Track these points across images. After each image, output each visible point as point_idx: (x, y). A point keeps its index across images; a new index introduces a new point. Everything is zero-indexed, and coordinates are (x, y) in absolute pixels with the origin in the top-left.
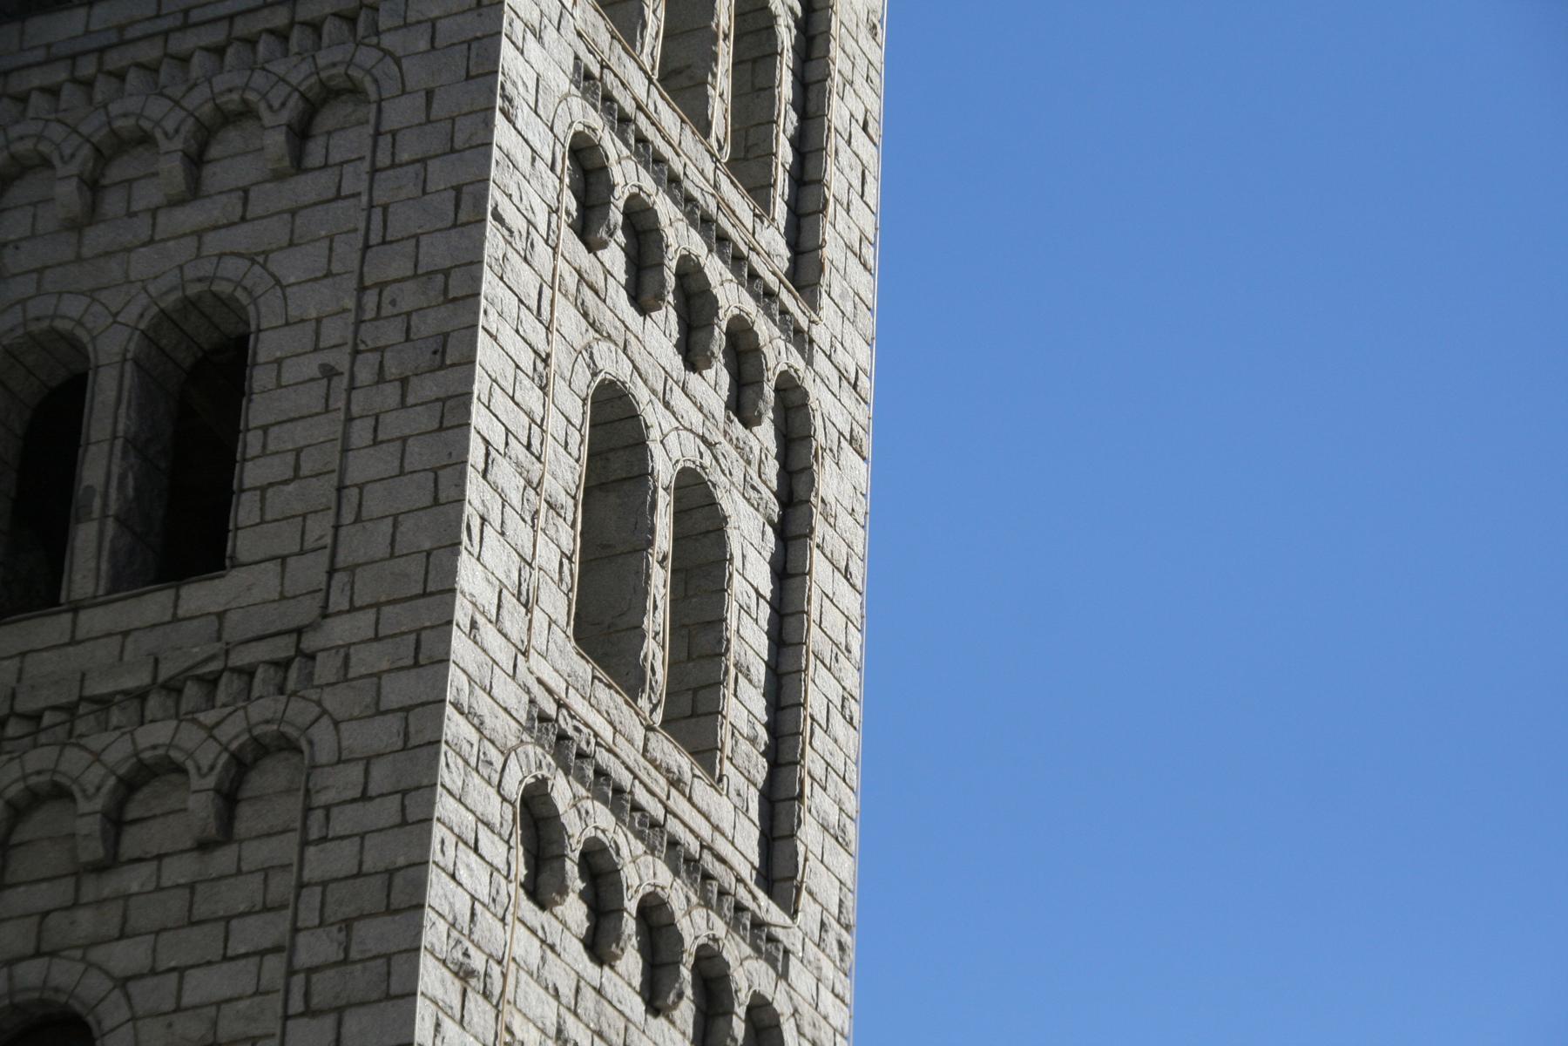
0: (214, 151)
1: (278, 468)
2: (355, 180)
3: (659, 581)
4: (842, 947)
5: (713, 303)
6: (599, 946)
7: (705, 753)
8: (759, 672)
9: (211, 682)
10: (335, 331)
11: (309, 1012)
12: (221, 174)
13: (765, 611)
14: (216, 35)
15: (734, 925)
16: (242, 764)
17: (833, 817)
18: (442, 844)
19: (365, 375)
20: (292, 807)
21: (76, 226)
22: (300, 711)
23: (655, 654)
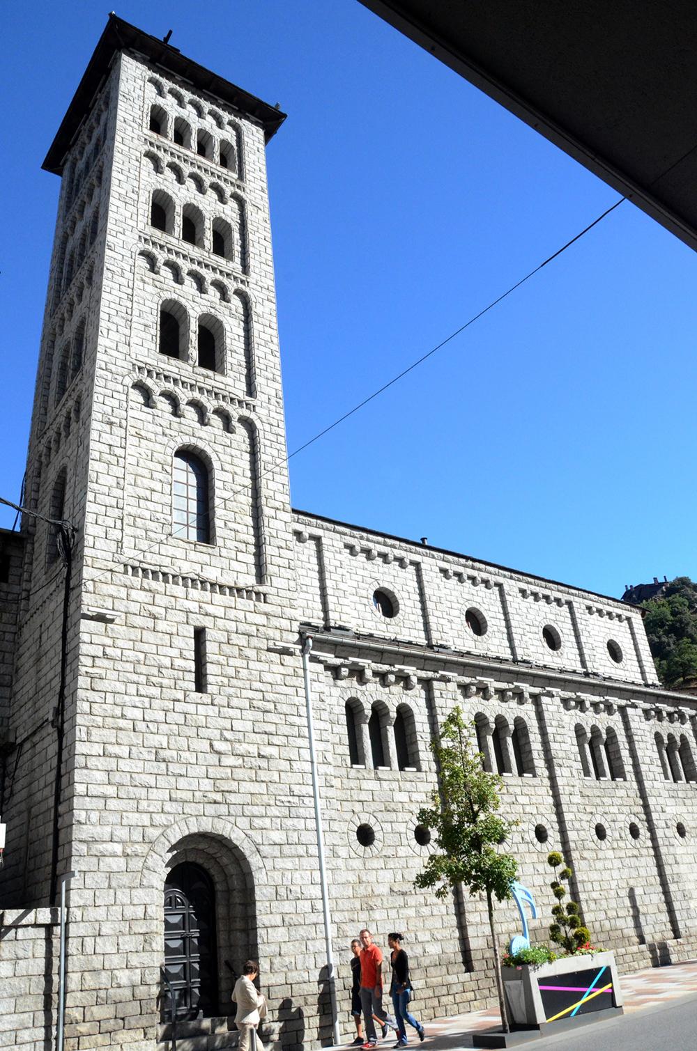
4: (278, 403)
5: (204, 278)
13: (242, 339)
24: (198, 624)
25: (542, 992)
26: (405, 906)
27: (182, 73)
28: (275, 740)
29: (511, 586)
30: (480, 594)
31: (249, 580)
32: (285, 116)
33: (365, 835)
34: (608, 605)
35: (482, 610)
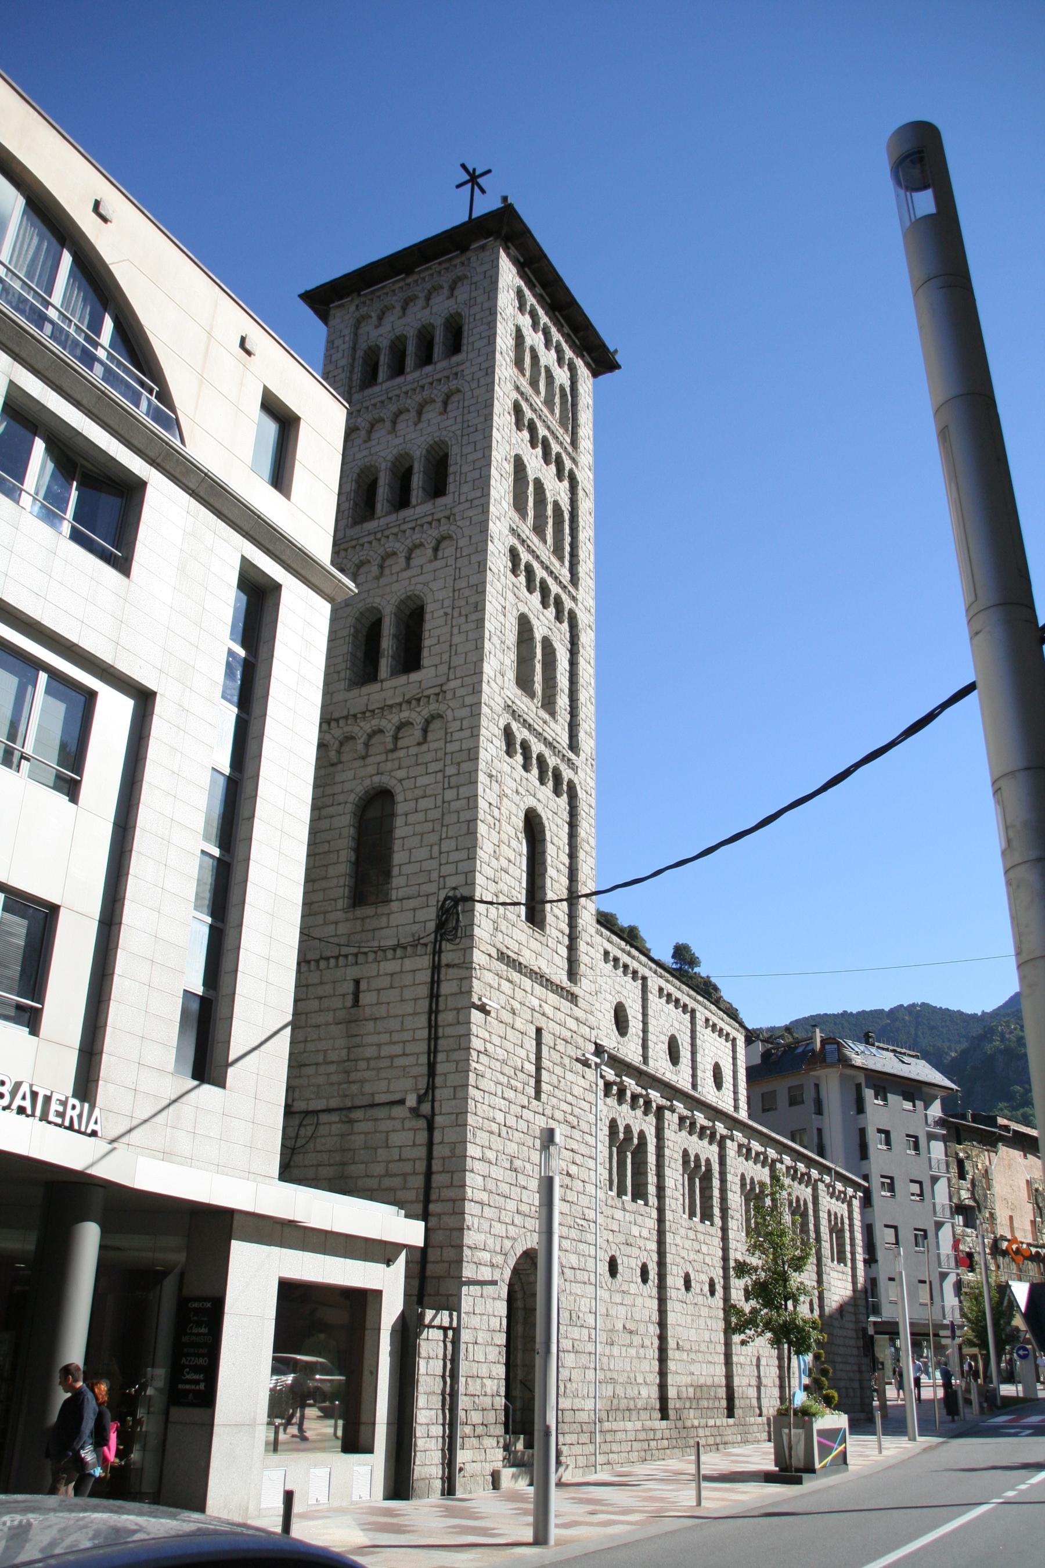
0: (413, 555)
1: (434, 641)
2: (451, 561)
3: (539, 668)
5: (550, 591)
6: (526, 767)
7: (553, 714)
8: (567, 691)
9: (419, 700)
10: (447, 603)
11: (450, 788)
12: (414, 562)
13: (567, 674)
14: (412, 524)
15: (563, 760)
16: (428, 722)
17: (588, 730)
18: (483, 742)
19: (456, 614)
20: (442, 733)
21: (377, 578)
22: (443, 707)
23: (538, 688)
24: (539, 1025)
25: (819, 1442)
26: (630, 1345)
27: (544, 286)
28: (578, 1159)
29: (655, 982)
30: (628, 986)
31: (560, 976)
32: (618, 367)
33: (613, 1268)
34: (722, 1019)
35: (627, 1006)
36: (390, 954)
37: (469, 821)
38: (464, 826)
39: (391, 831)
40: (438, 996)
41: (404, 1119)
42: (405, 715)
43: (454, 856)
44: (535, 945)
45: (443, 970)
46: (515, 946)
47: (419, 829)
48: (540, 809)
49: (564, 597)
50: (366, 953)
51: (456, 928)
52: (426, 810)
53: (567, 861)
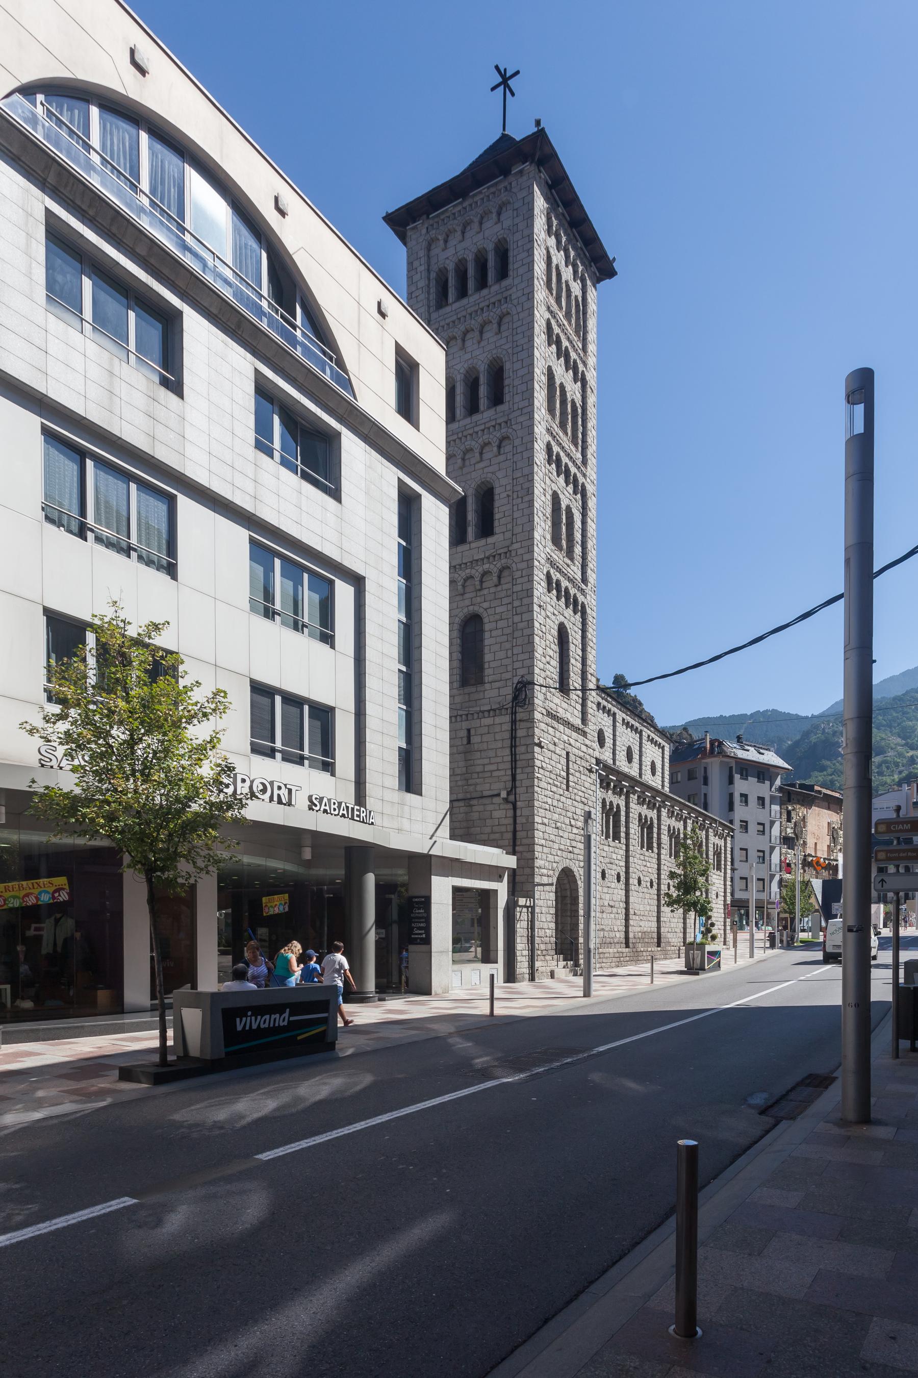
0: (484, 451)
1: (501, 515)
2: (510, 456)
3: (564, 528)
6: (558, 598)
7: (572, 559)
8: (580, 542)
9: (494, 556)
10: (508, 488)
11: (516, 614)
12: (485, 456)
14: (482, 427)
15: (578, 590)
16: (501, 571)
17: (592, 568)
18: (536, 585)
19: (515, 497)
20: (510, 579)
21: (461, 468)
22: (510, 561)
23: (564, 543)
31: (577, 722)
36: (486, 714)
37: (529, 635)
38: (526, 638)
39: (482, 640)
40: (515, 738)
41: (500, 804)
42: (486, 566)
43: (521, 657)
44: (565, 705)
45: (518, 723)
46: (554, 707)
47: (499, 640)
48: (566, 622)
49: (579, 475)
50: (472, 714)
51: (525, 700)
52: (502, 628)
53: (580, 653)
